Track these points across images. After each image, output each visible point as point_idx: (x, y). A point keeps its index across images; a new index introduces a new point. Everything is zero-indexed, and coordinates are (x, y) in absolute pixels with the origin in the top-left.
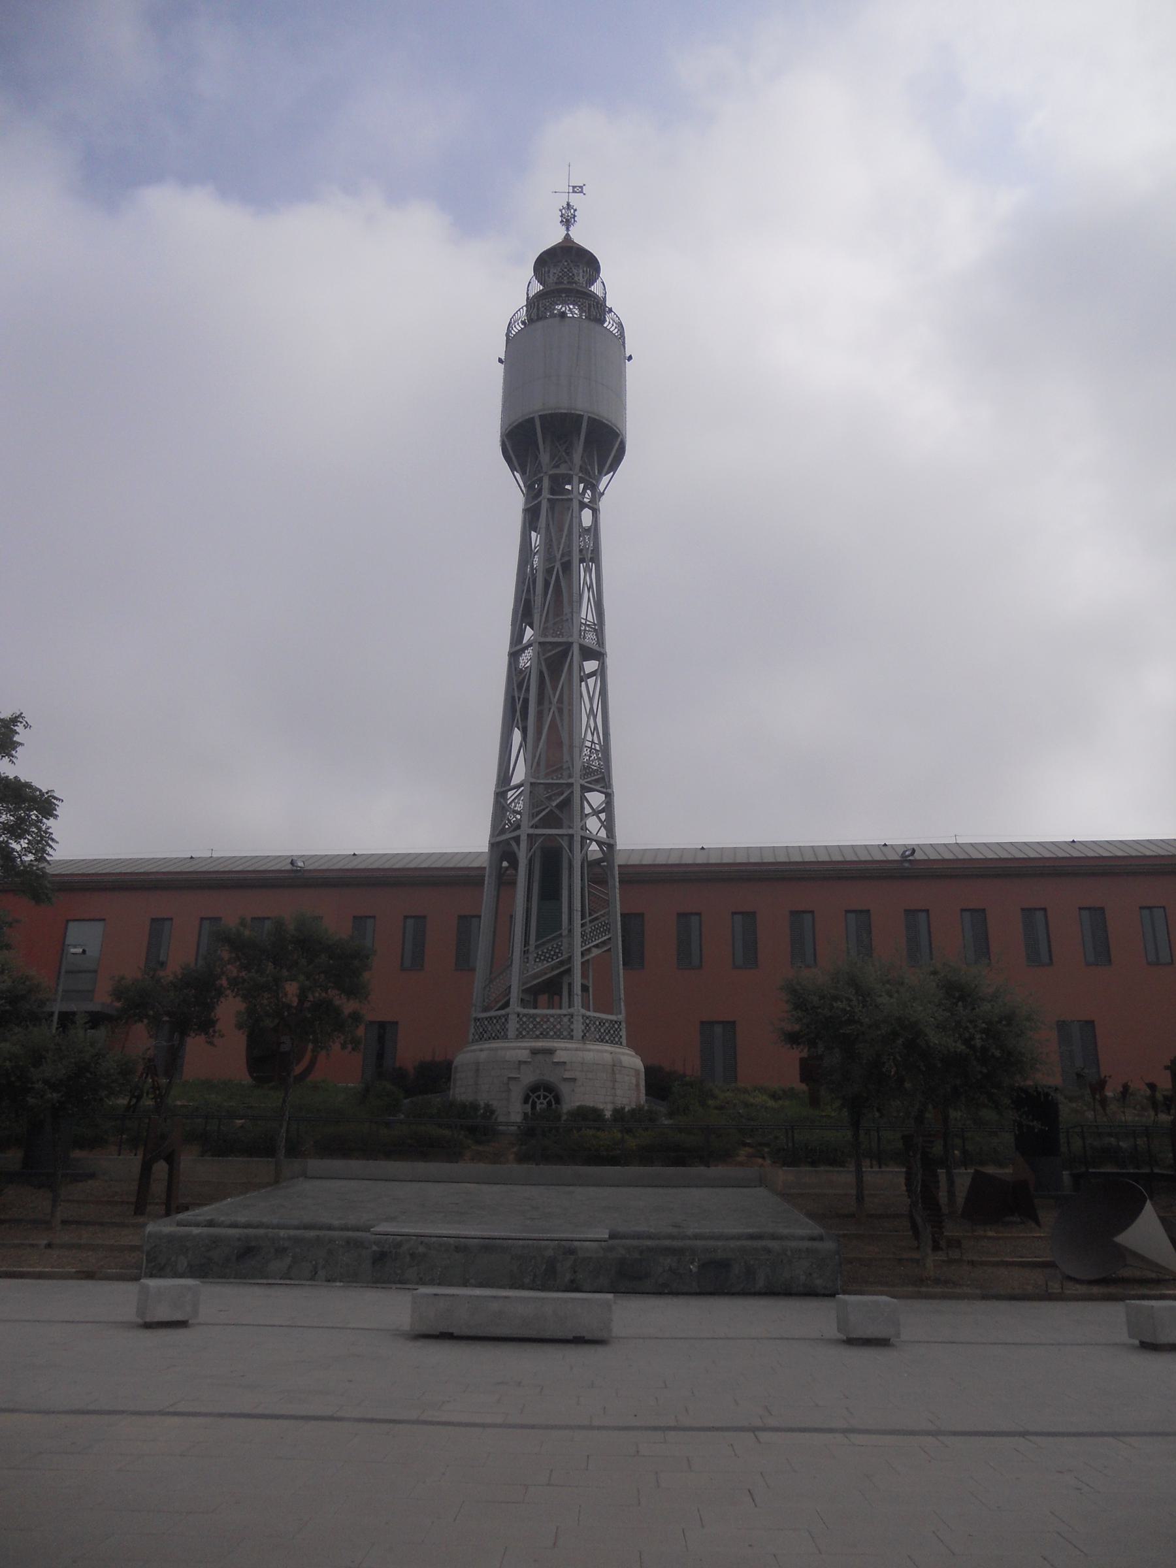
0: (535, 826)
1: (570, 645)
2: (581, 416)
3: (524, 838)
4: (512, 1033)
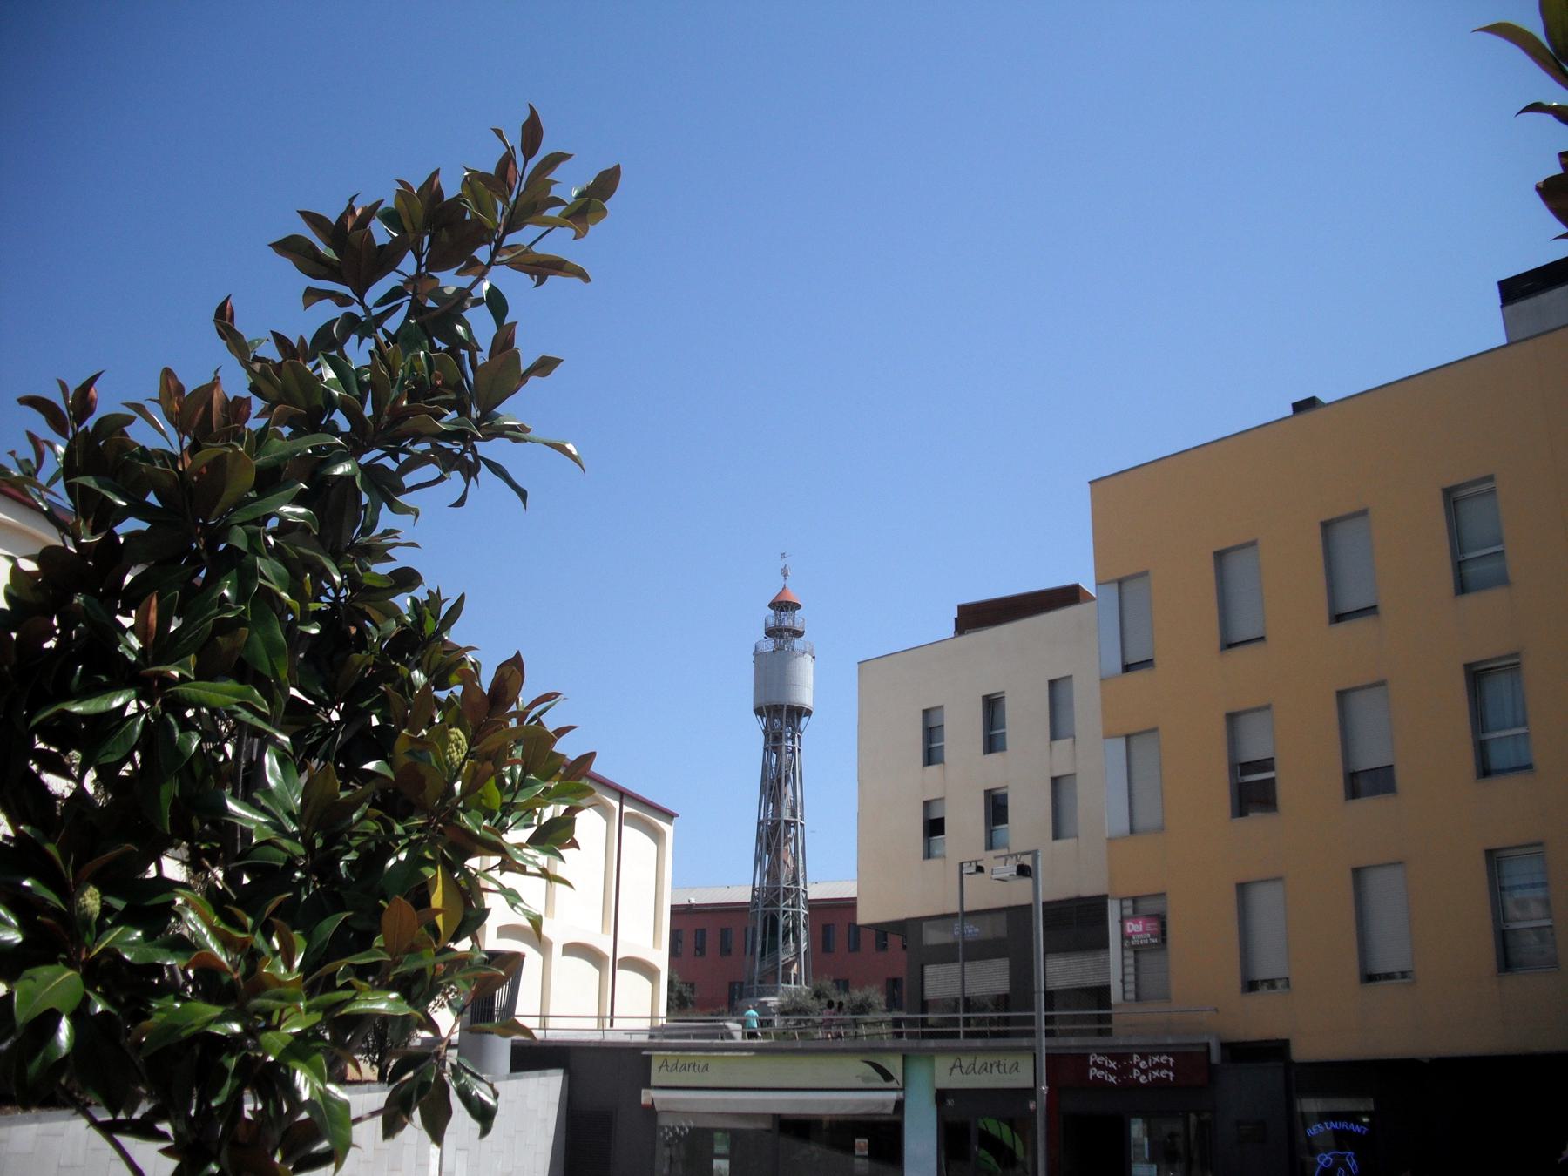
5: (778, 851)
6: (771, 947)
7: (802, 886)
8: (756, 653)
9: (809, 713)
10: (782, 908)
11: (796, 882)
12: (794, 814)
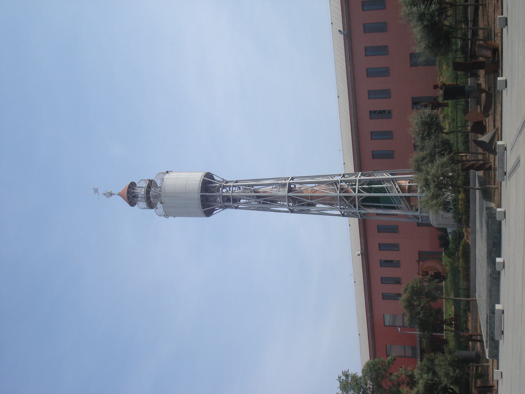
0: (355, 206)
1: (289, 197)
2: (202, 196)
3: (360, 211)
4: (427, 215)
5: (312, 198)
6: (388, 203)
7: (339, 178)
8: (167, 215)
9: (209, 175)
10: (356, 194)
11: (336, 183)
12: (284, 185)
